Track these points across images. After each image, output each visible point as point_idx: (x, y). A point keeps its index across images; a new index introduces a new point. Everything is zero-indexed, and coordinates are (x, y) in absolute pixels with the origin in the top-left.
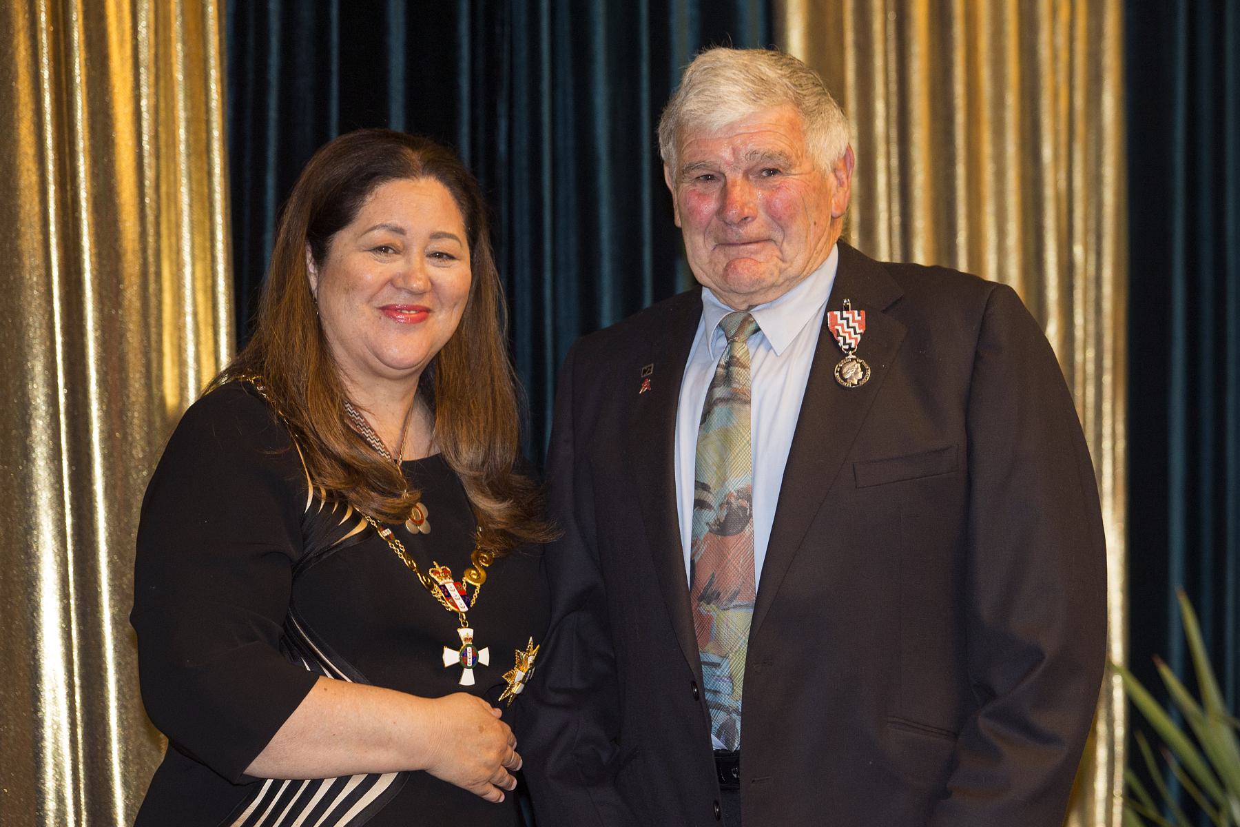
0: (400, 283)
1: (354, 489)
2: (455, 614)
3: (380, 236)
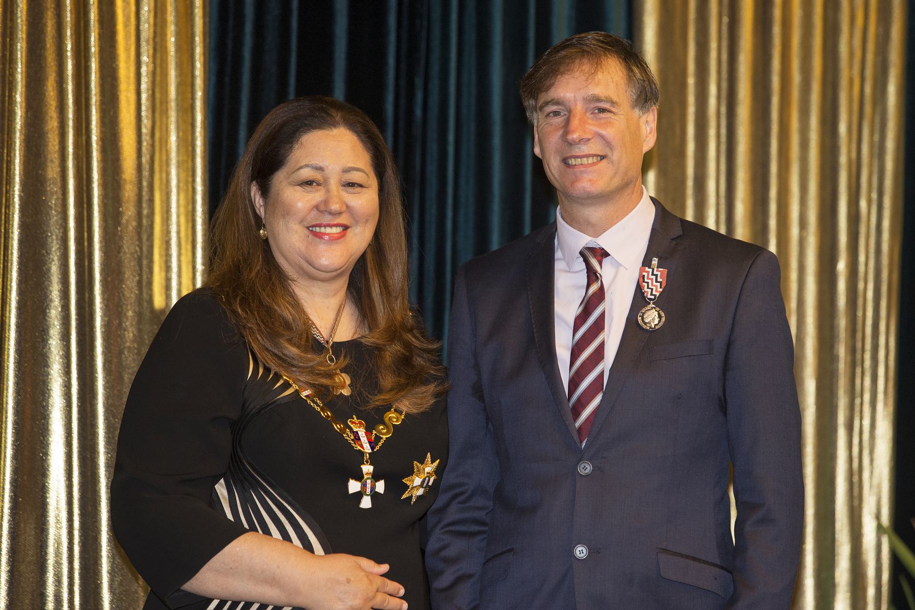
0: (322, 208)
3: (306, 173)
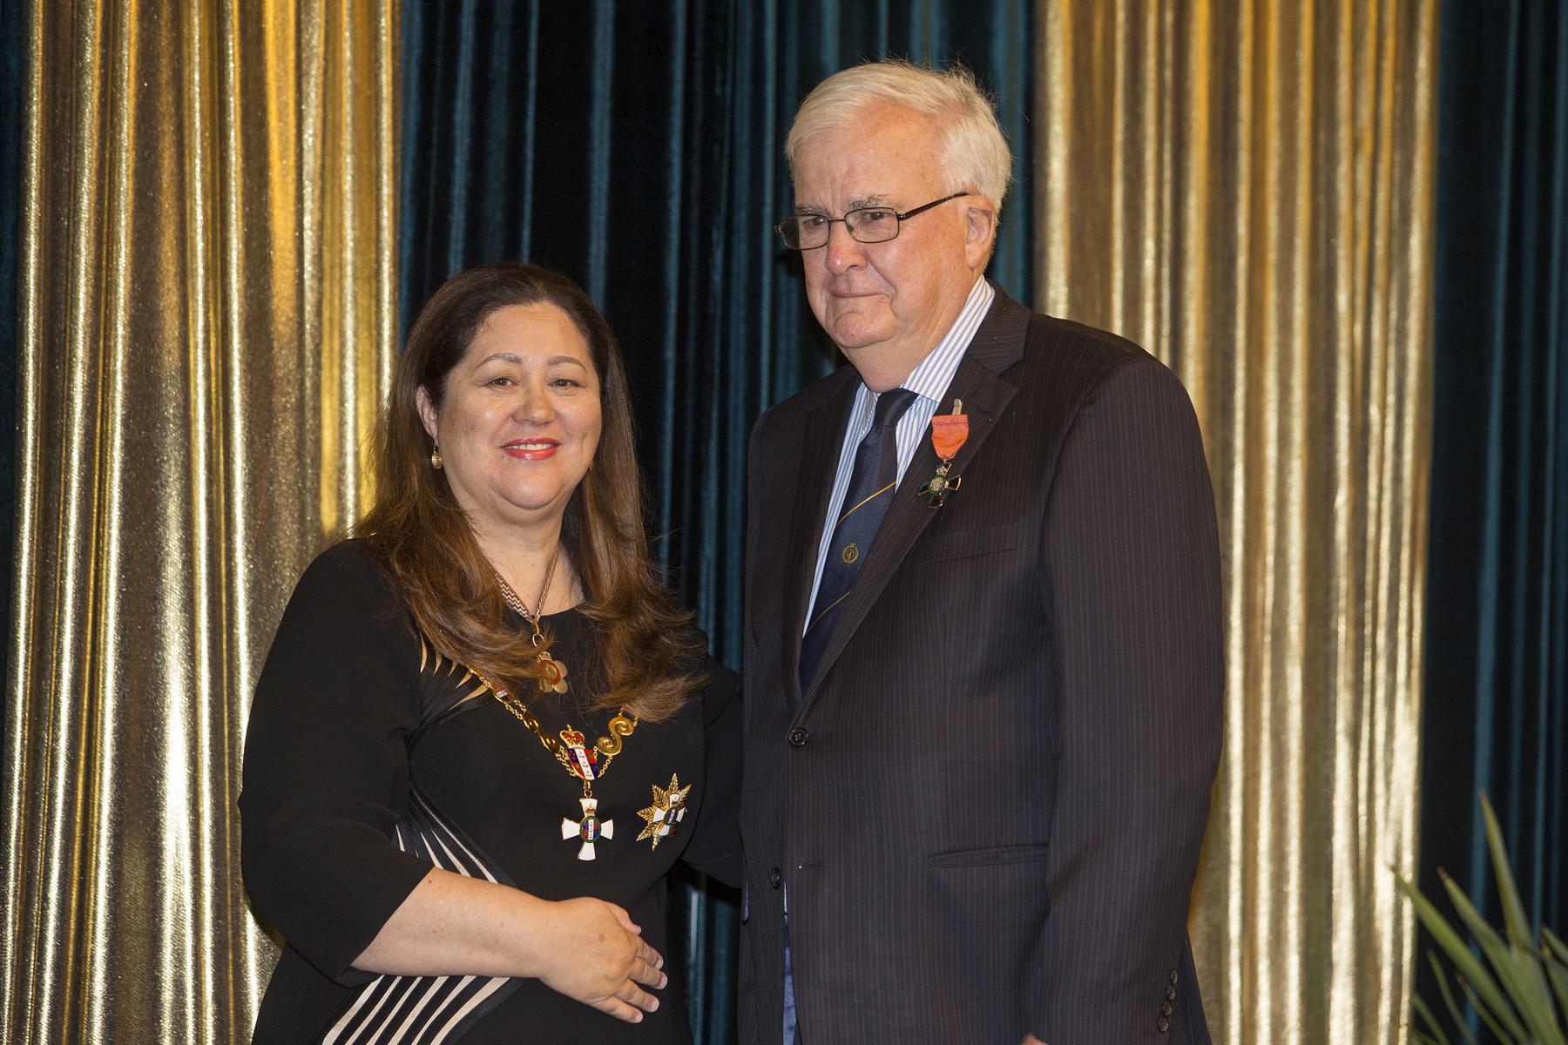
0: (521, 417)
2: (580, 781)
3: (496, 367)
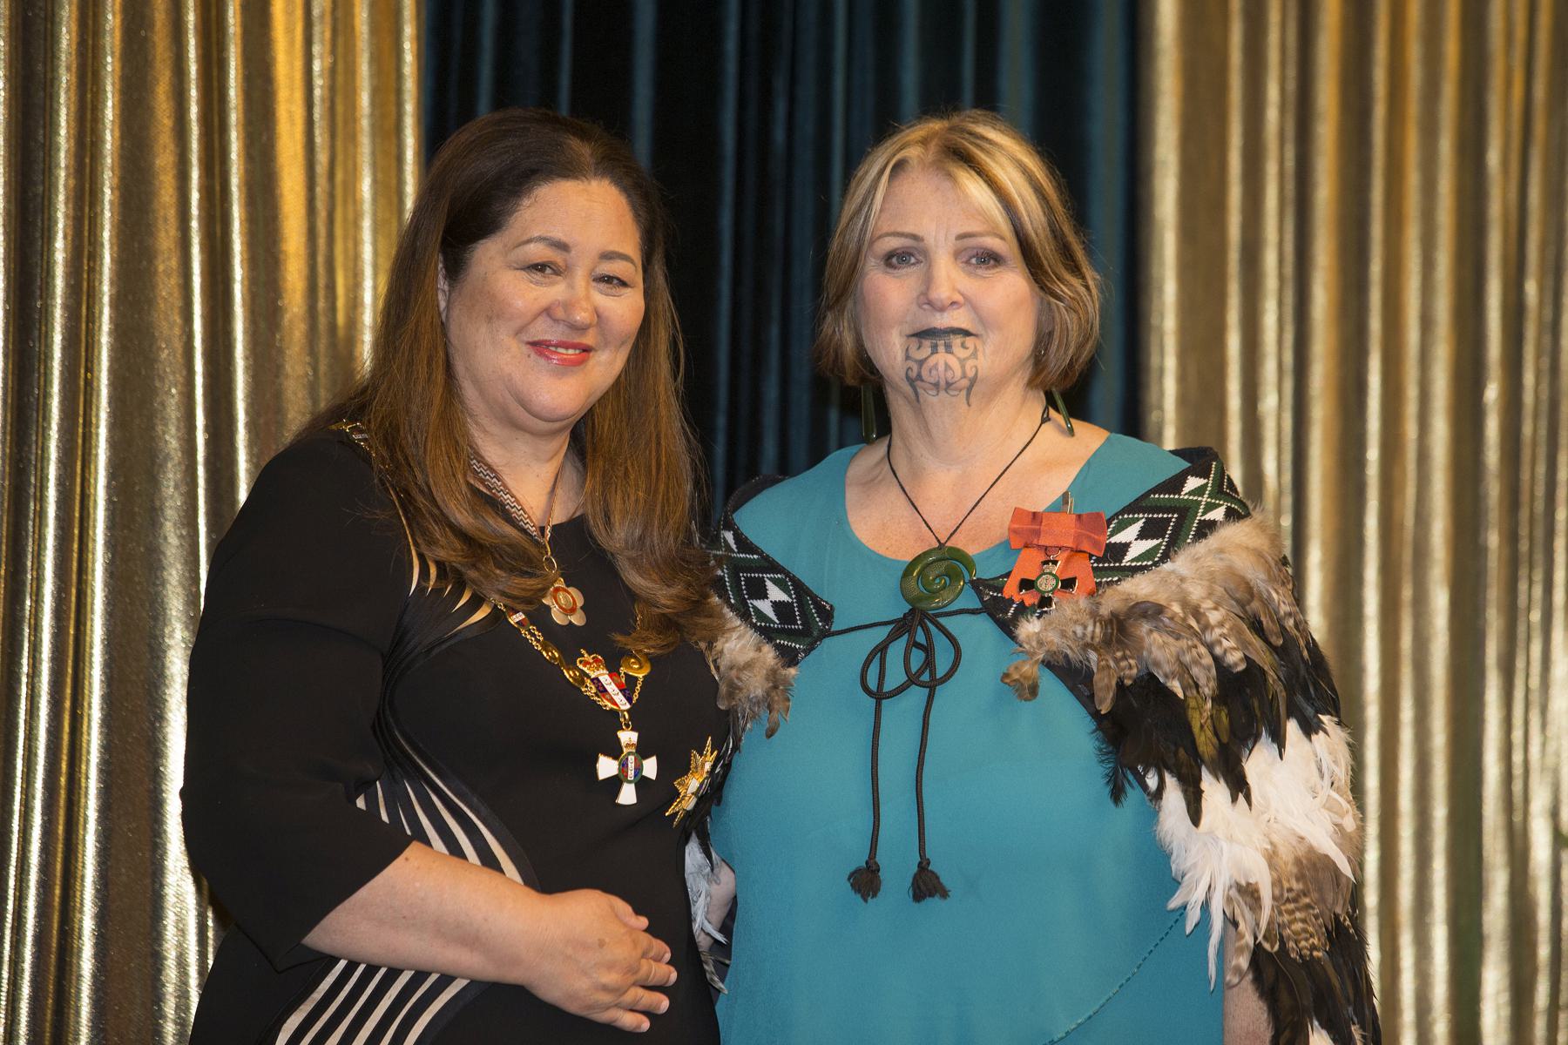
0: (560, 313)
1: (474, 566)
2: (615, 714)
3: (537, 252)
